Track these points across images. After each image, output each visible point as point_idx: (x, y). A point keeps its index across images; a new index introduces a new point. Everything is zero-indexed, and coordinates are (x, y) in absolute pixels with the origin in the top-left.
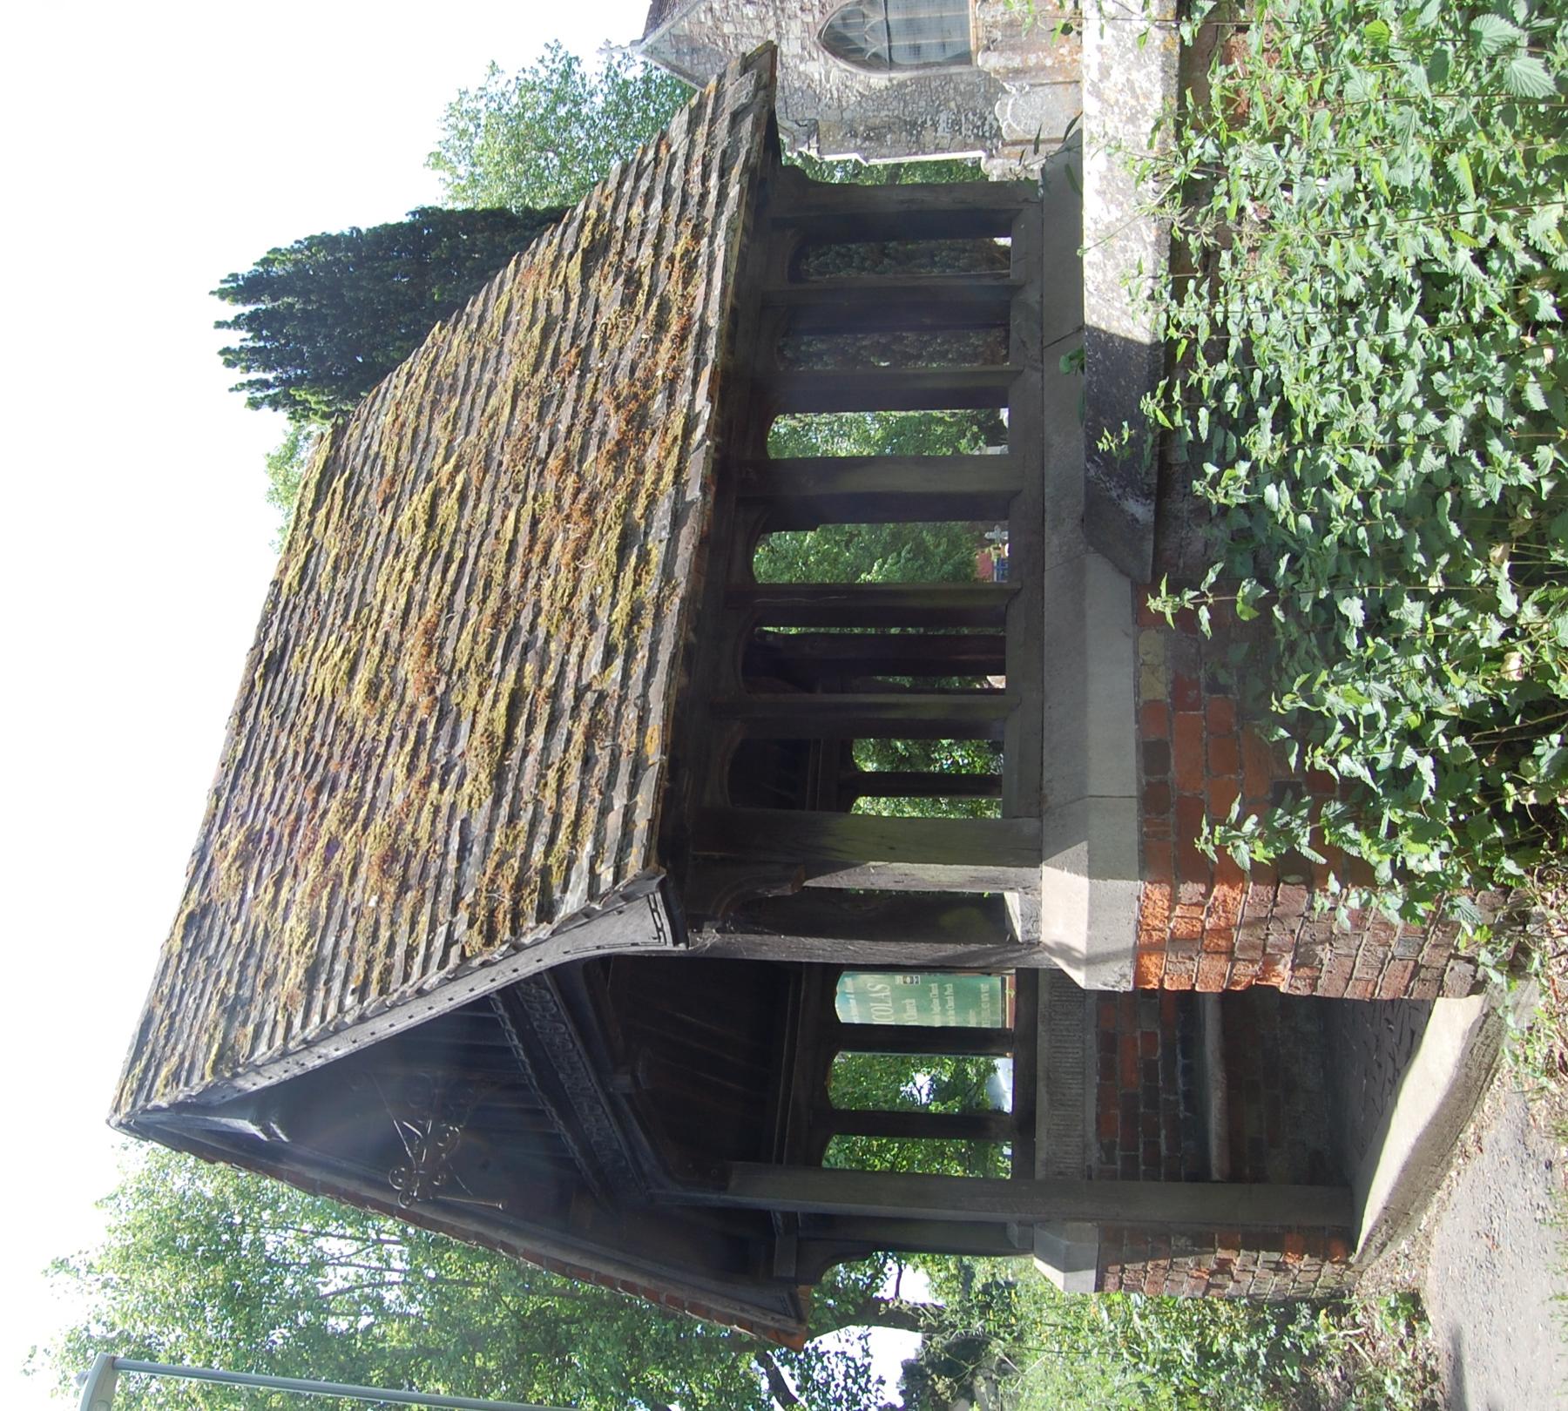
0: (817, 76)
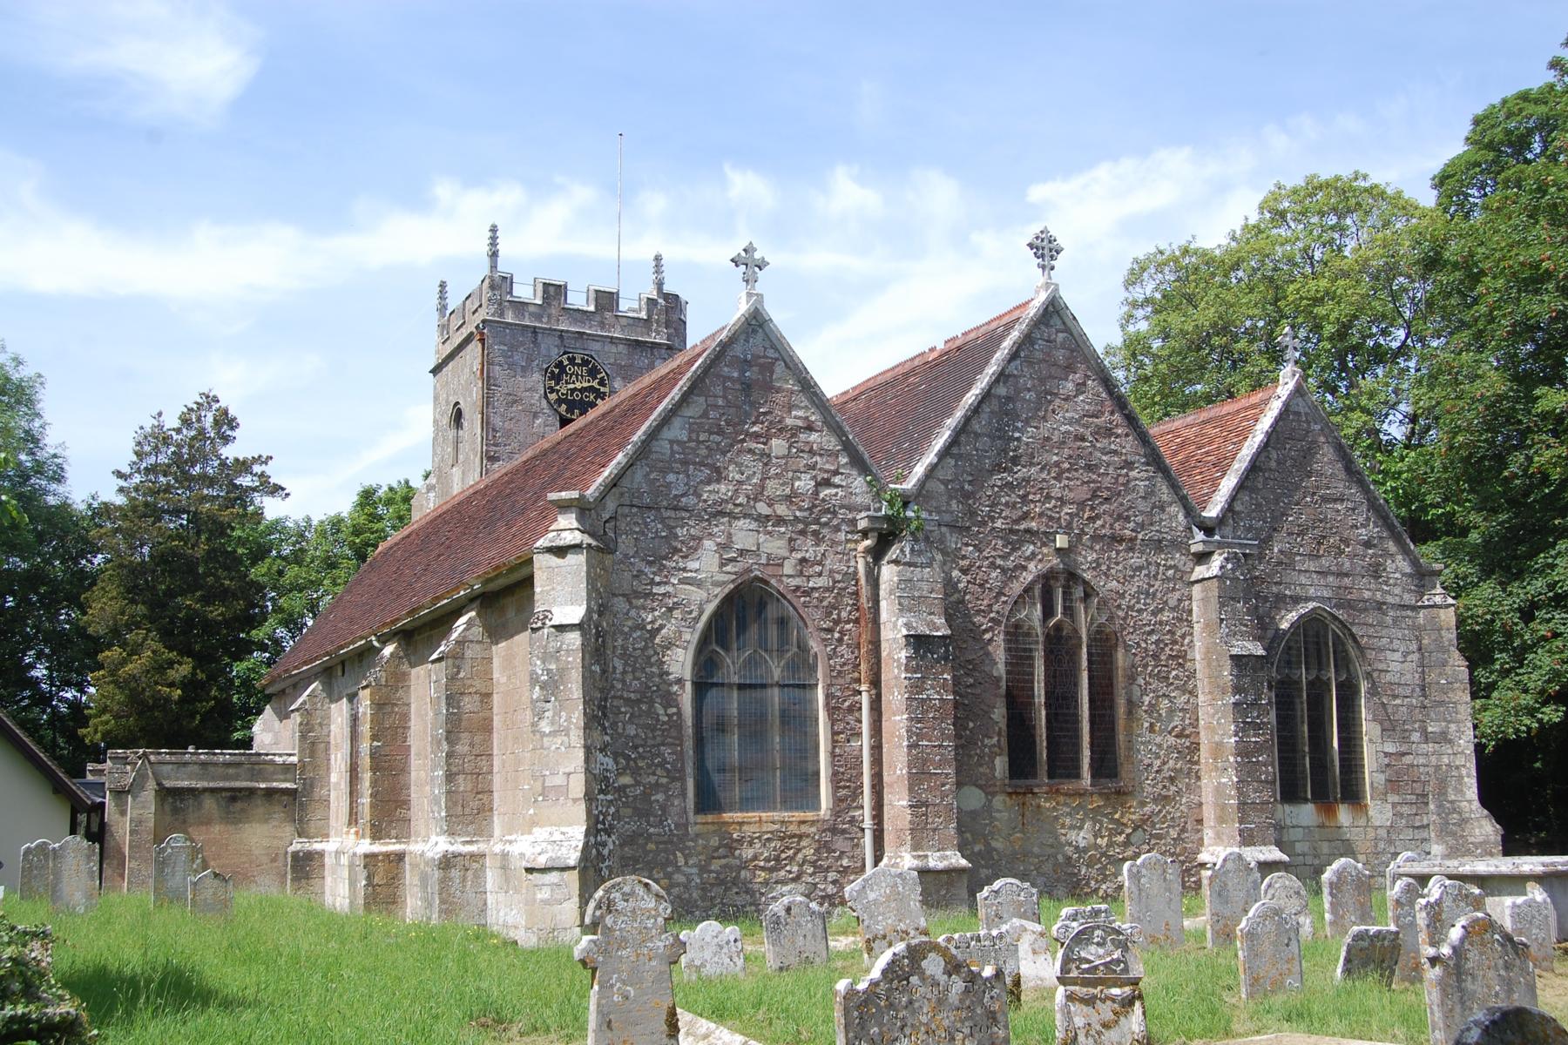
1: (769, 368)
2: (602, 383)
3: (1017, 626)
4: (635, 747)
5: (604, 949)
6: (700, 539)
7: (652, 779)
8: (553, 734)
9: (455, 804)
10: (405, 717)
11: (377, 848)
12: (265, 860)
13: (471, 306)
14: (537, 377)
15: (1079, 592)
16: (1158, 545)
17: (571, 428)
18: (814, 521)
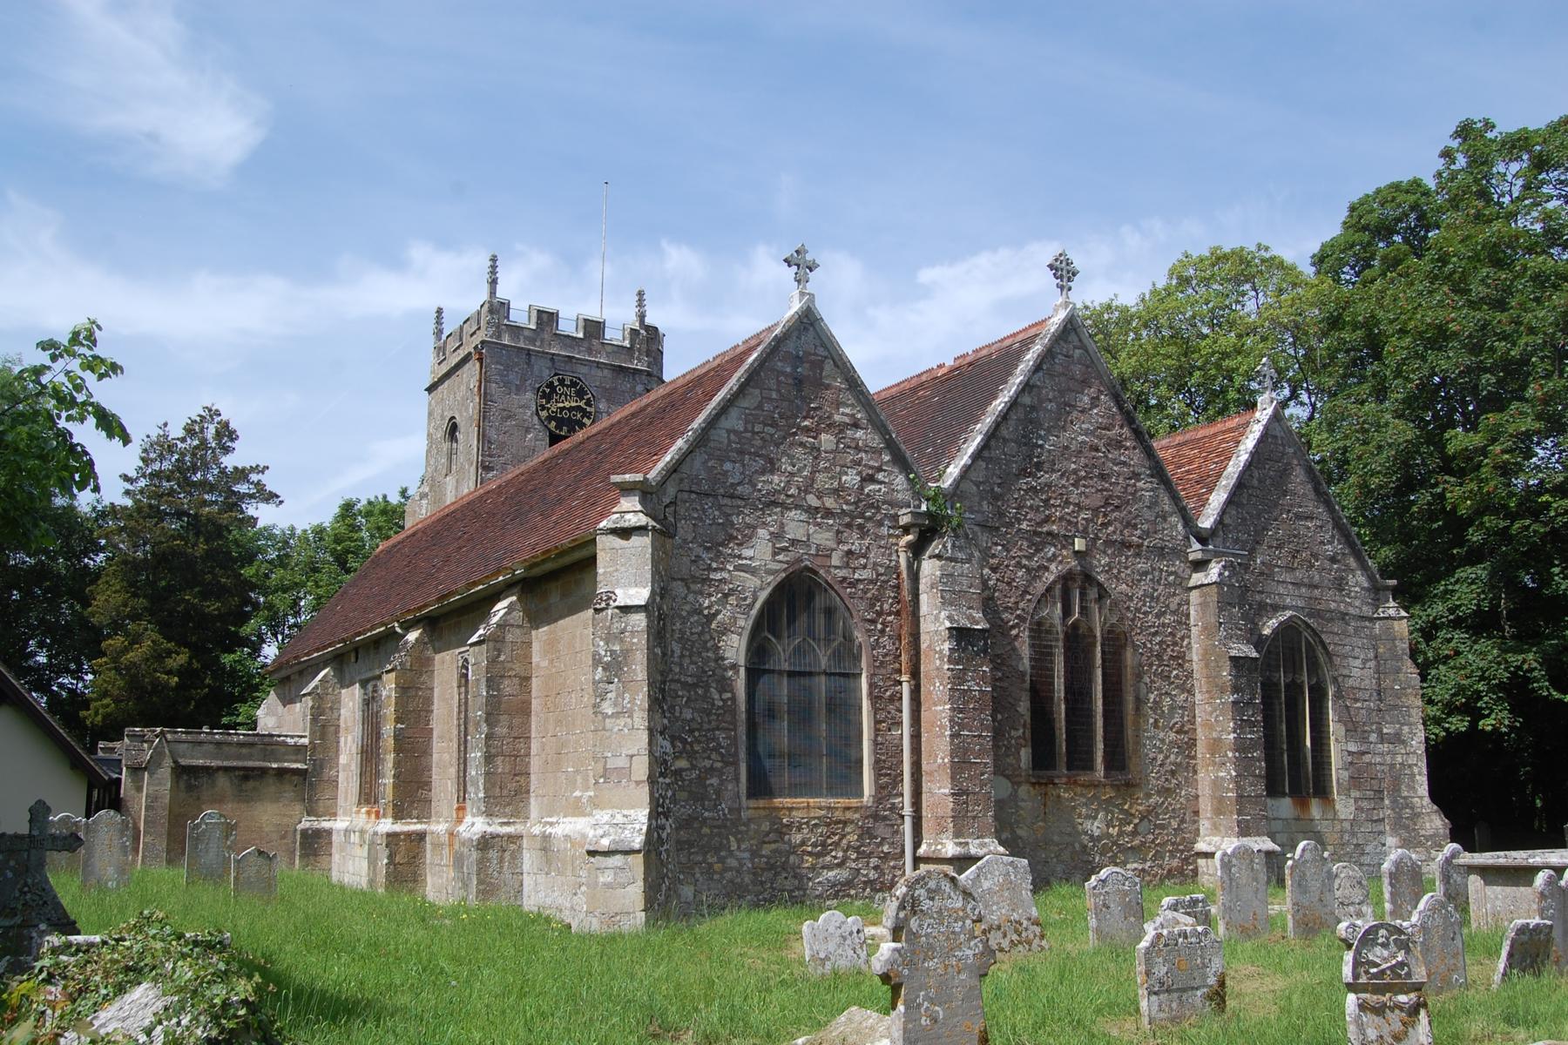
0: (748, 553)
1: (818, 365)
2: (588, 403)
3: (1039, 624)
4: (691, 731)
5: (908, 958)
6: (755, 527)
7: (707, 763)
8: (616, 715)
9: (494, 785)
10: (429, 701)
11: (399, 827)
12: (275, 836)
13: (469, 329)
14: (529, 395)
15: (1093, 593)
16: (1161, 552)
17: (563, 445)
18: (859, 515)
